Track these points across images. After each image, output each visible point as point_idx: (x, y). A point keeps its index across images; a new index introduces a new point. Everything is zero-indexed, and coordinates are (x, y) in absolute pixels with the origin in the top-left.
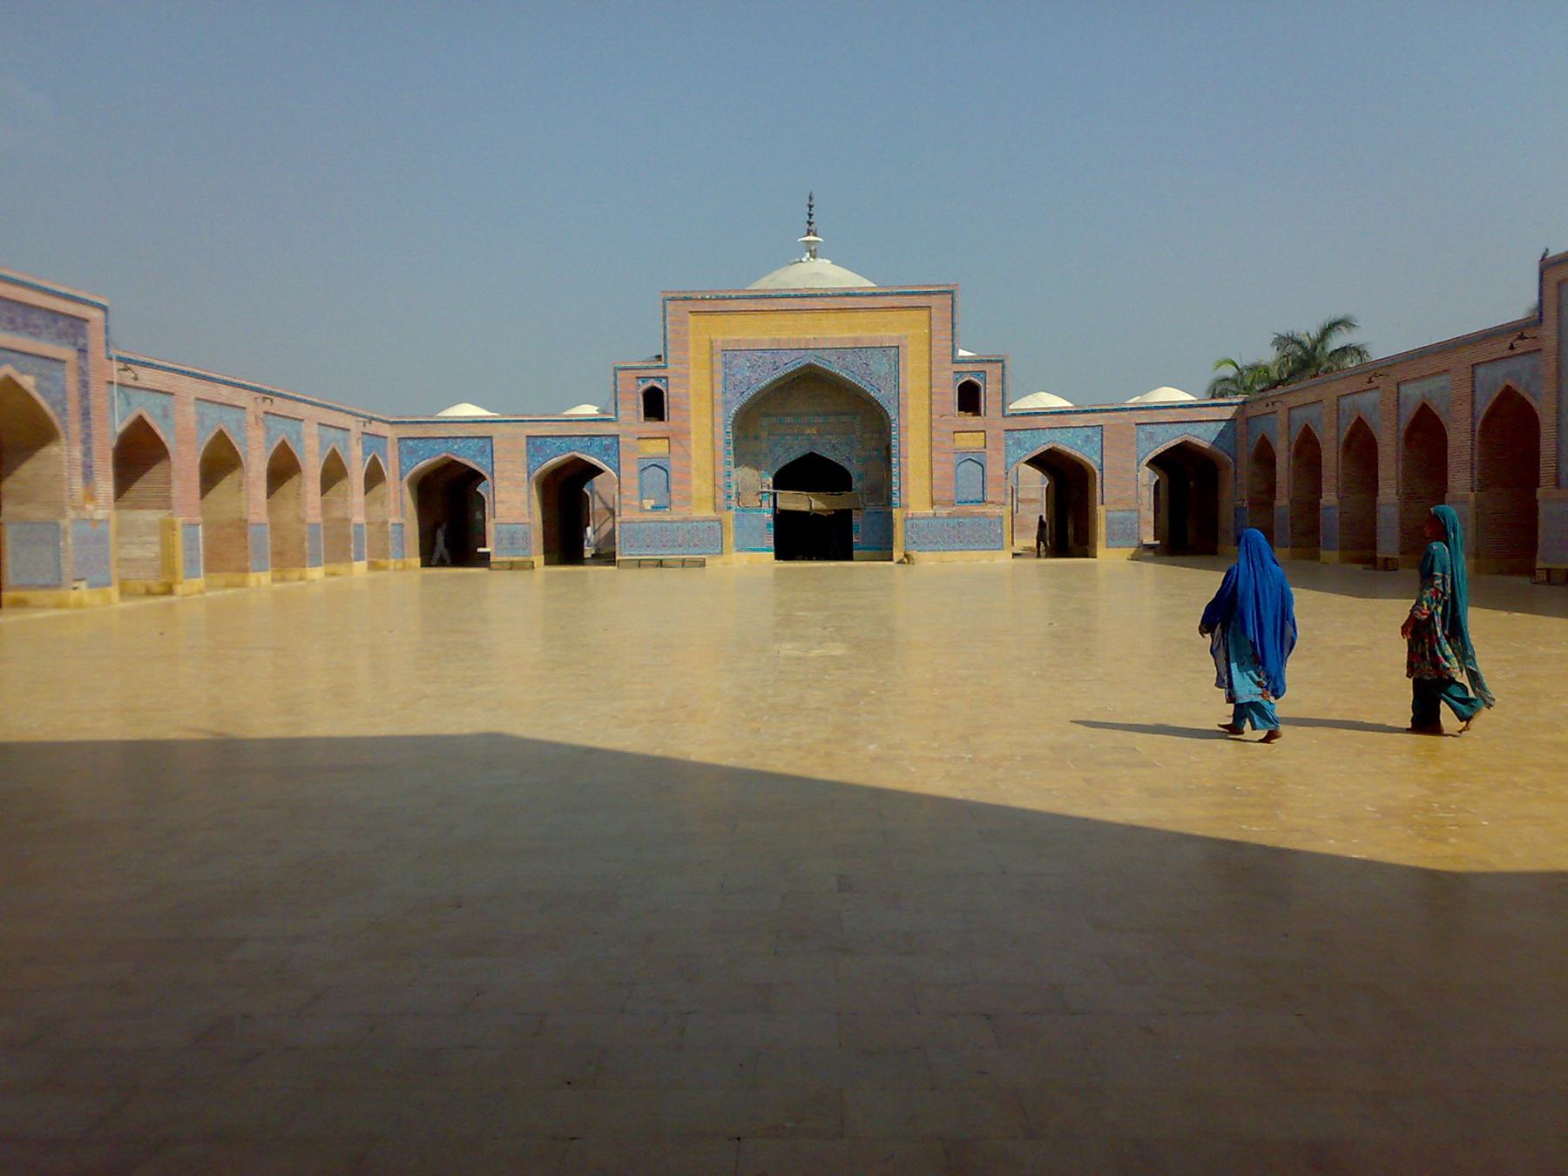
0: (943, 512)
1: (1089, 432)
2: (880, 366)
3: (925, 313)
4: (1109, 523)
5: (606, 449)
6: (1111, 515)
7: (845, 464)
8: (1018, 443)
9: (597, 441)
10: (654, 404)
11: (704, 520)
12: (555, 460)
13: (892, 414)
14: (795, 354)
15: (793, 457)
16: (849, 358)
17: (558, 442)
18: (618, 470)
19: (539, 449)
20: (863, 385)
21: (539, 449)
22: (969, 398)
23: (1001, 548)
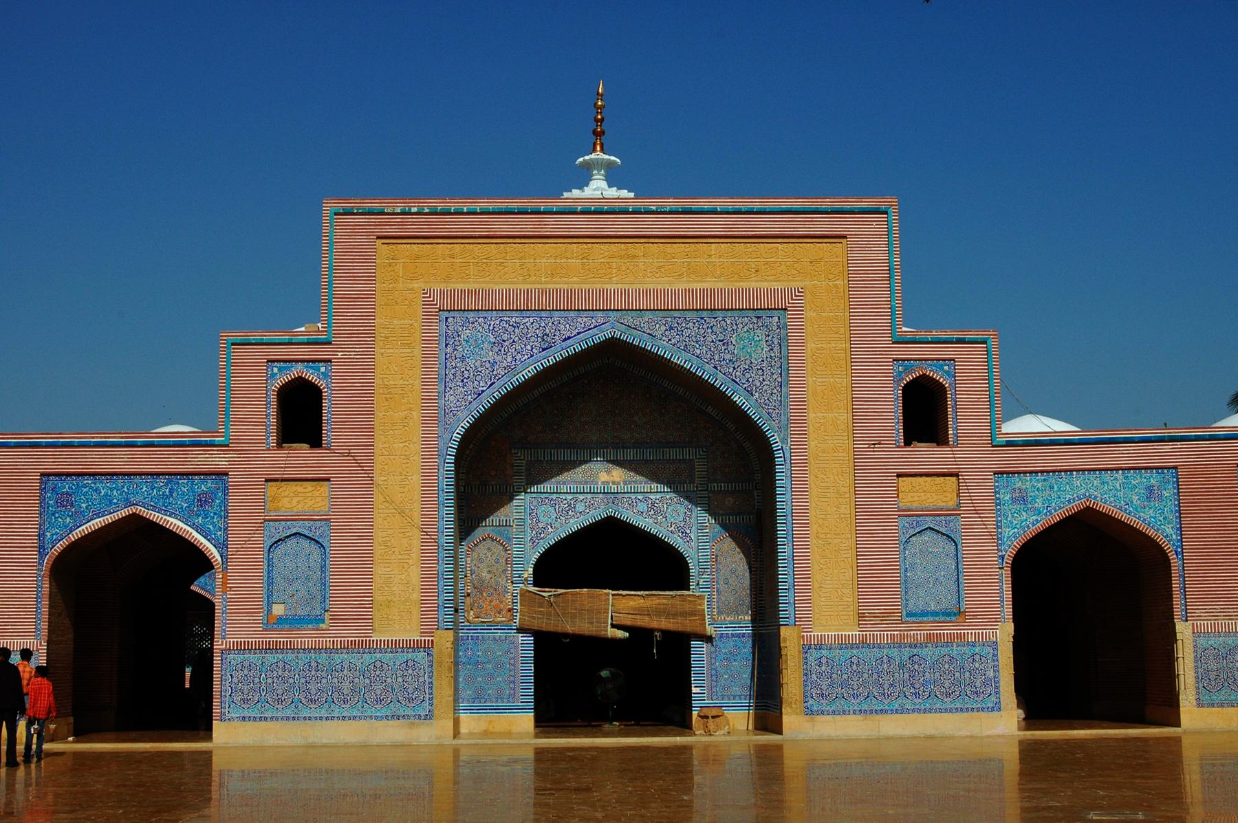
0: (881, 633)
1: (1154, 479)
2: (751, 345)
3: (837, 248)
4: (1200, 656)
5: (203, 501)
6: (1203, 642)
7: (676, 541)
8: (1022, 499)
9: (184, 485)
10: (300, 415)
11: (395, 647)
12: (97, 523)
13: (775, 439)
14: (583, 320)
15: (574, 525)
16: (692, 329)
17: (104, 487)
18: (222, 546)
19: (65, 501)
20: (720, 381)
21: (65, 501)
22: (924, 412)
23: (997, 708)
